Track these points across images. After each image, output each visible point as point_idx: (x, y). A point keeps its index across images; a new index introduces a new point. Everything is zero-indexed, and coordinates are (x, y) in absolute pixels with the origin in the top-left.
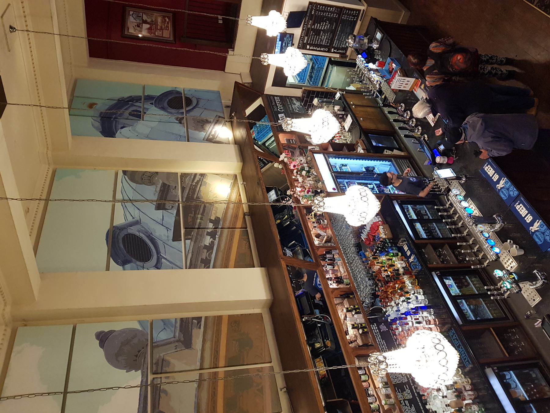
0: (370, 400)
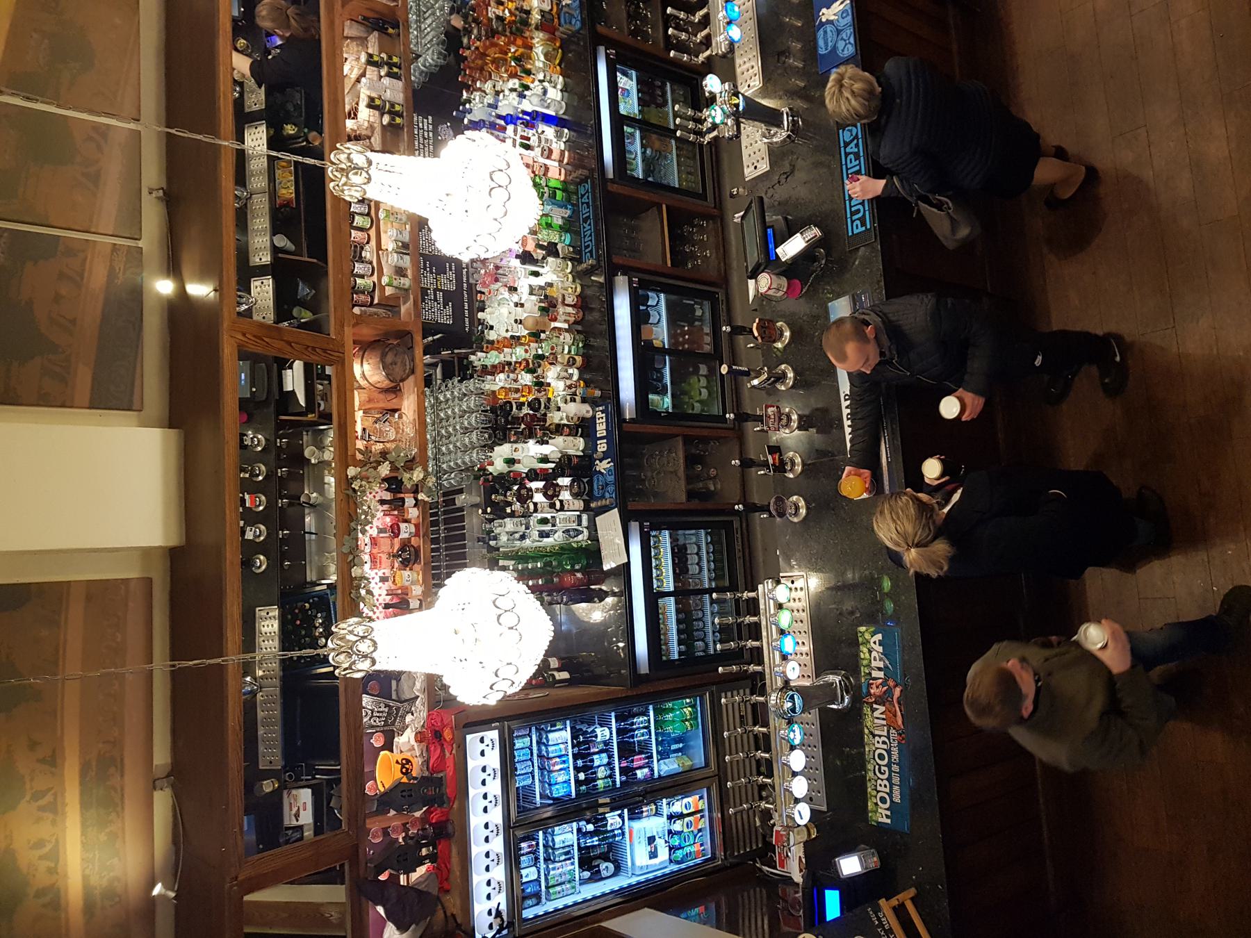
0: (359, 268)
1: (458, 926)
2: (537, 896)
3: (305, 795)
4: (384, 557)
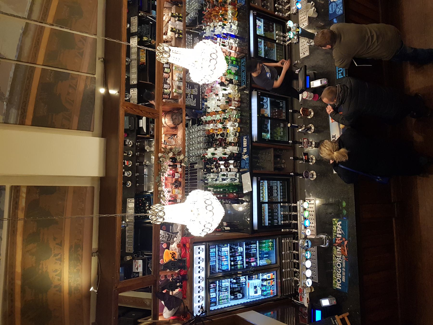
0: (165, 86)
1: (188, 310)
2: (215, 303)
3: (140, 262)
4: (169, 184)
